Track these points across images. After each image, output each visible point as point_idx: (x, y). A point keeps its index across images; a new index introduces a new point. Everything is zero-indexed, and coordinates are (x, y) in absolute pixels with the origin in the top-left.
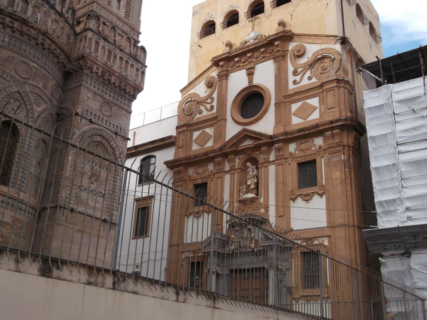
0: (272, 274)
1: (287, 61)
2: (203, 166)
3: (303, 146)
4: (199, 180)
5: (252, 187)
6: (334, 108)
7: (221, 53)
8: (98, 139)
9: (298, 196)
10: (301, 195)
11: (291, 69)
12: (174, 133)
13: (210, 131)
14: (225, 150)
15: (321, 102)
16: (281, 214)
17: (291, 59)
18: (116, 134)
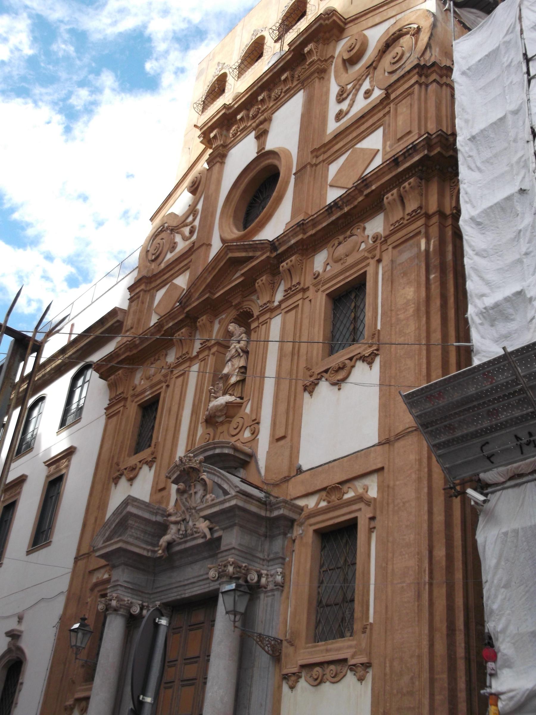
1: (329, 80)
3: (341, 250)
4: (148, 393)
5: (233, 380)
6: (409, 133)
10: (326, 371)
11: (334, 89)
14: (190, 304)
16: (280, 433)
17: (336, 72)
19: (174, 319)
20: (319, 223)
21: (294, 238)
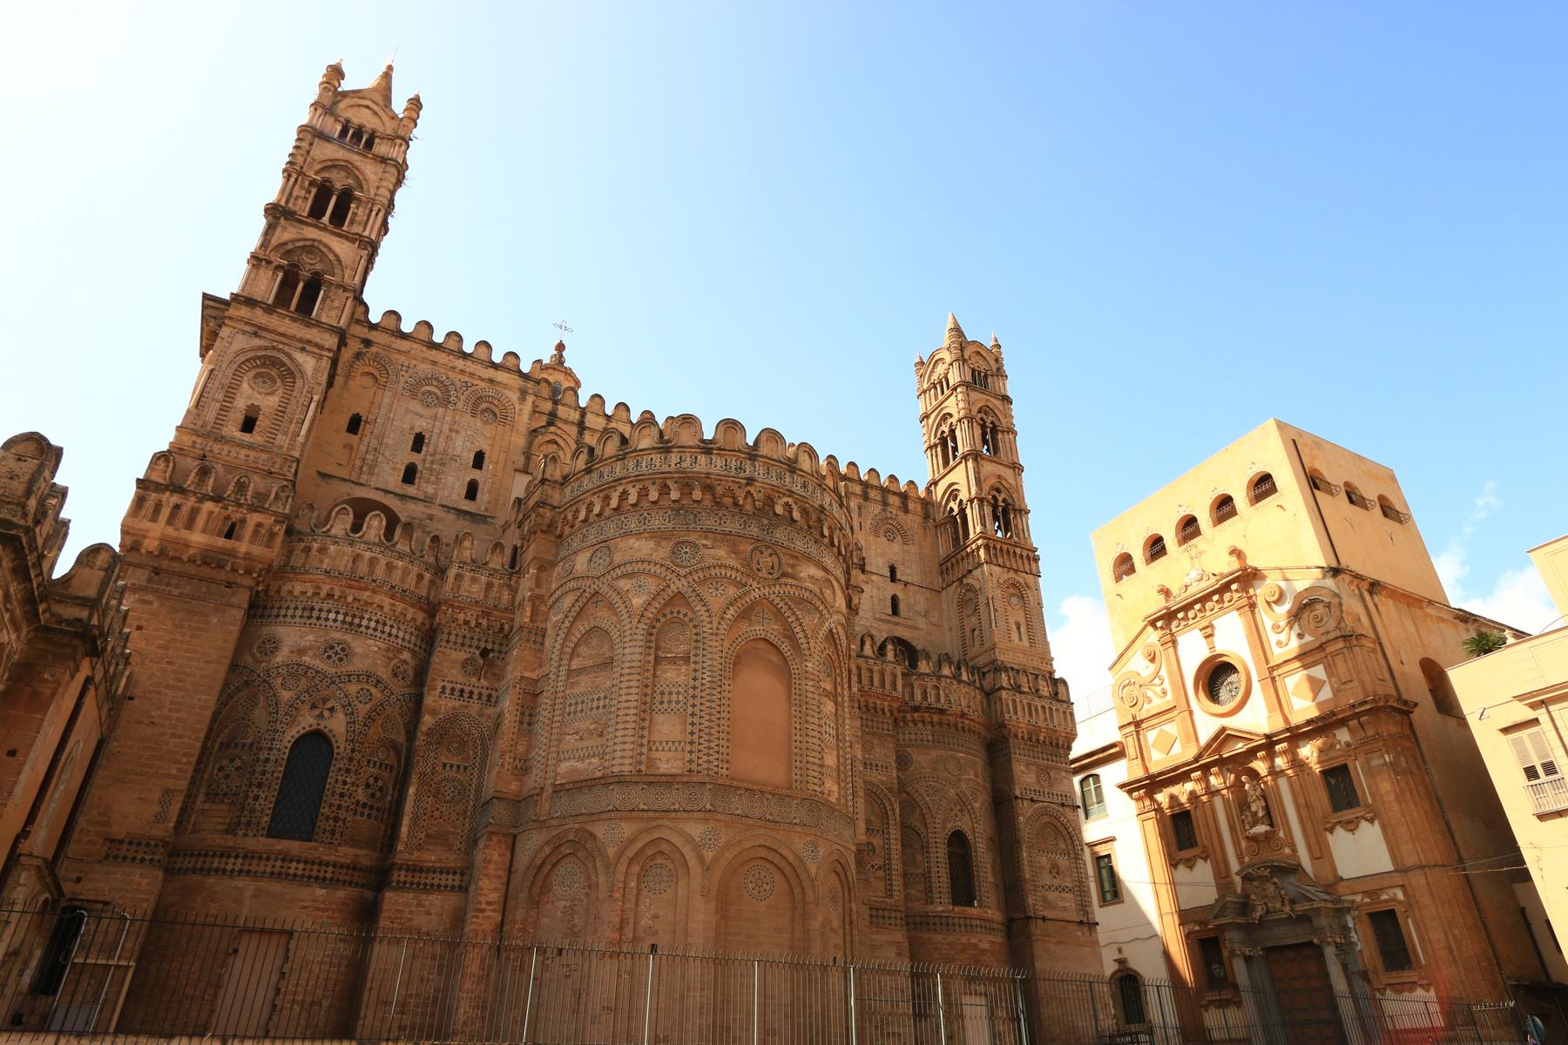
0: (1330, 952)
5: (1261, 814)
7: (1154, 609)
8: (1046, 819)
9: (1335, 825)
12: (1116, 736)
13: (1171, 729)
15: (1330, 671)
18: (1063, 805)
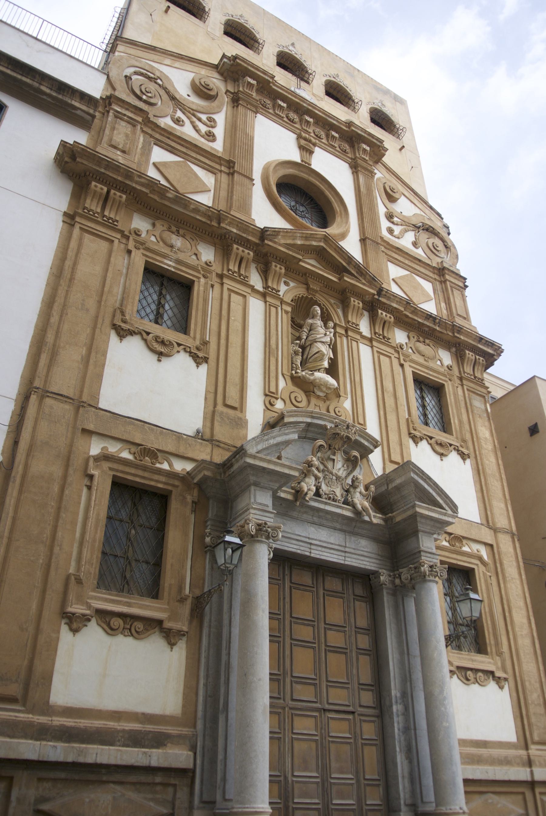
2: (183, 236)
3: (421, 347)
4: (170, 263)
10: (431, 438)
19: (239, 230)
20: (416, 315)
21: (397, 304)
